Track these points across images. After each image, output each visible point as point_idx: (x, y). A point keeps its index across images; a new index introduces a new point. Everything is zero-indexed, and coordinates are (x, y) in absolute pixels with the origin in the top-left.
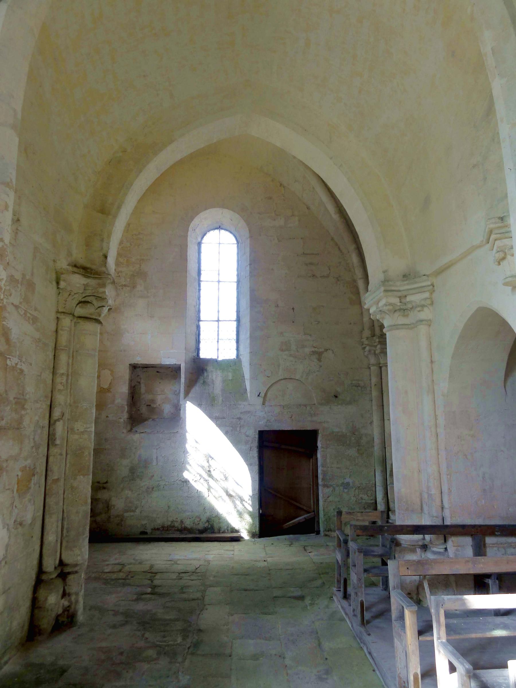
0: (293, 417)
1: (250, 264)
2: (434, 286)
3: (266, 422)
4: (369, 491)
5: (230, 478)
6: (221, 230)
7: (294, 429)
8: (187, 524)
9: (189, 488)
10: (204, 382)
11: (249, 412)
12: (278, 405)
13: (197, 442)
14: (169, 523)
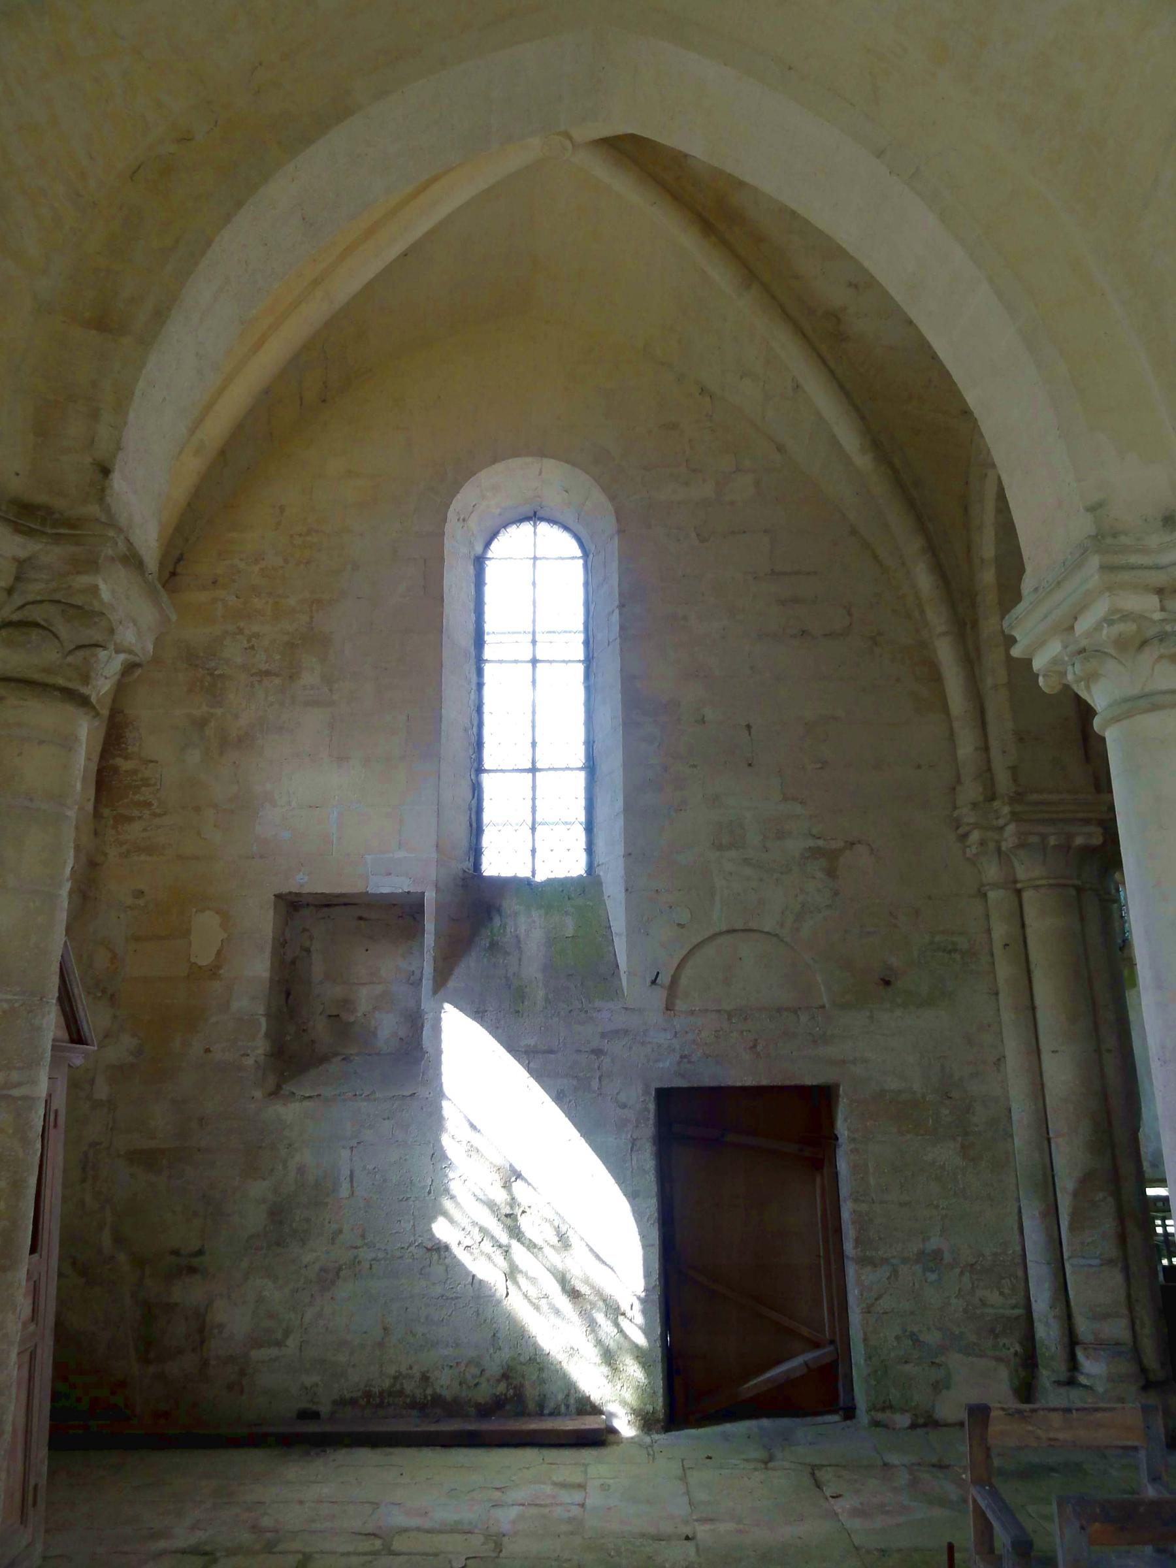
0: (759, 1048)
1: (622, 606)
3: (679, 1063)
4: (1004, 1278)
5: (574, 1240)
6: (538, 522)
8: (442, 1386)
9: (447, 1270)
10: (494, 947)
12: (714, 1011)
13: (473, 1127)
14: (387, 1383)
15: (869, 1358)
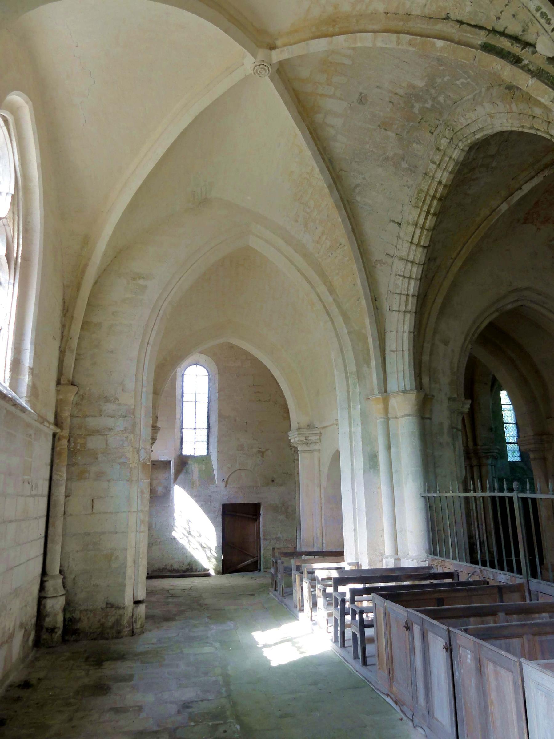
1: (218, 392)
2: (321, 433)
7: (246, 502)
10: (186, 472)
11: (216, 492)
14: (163, 567)
15: (264, 559)
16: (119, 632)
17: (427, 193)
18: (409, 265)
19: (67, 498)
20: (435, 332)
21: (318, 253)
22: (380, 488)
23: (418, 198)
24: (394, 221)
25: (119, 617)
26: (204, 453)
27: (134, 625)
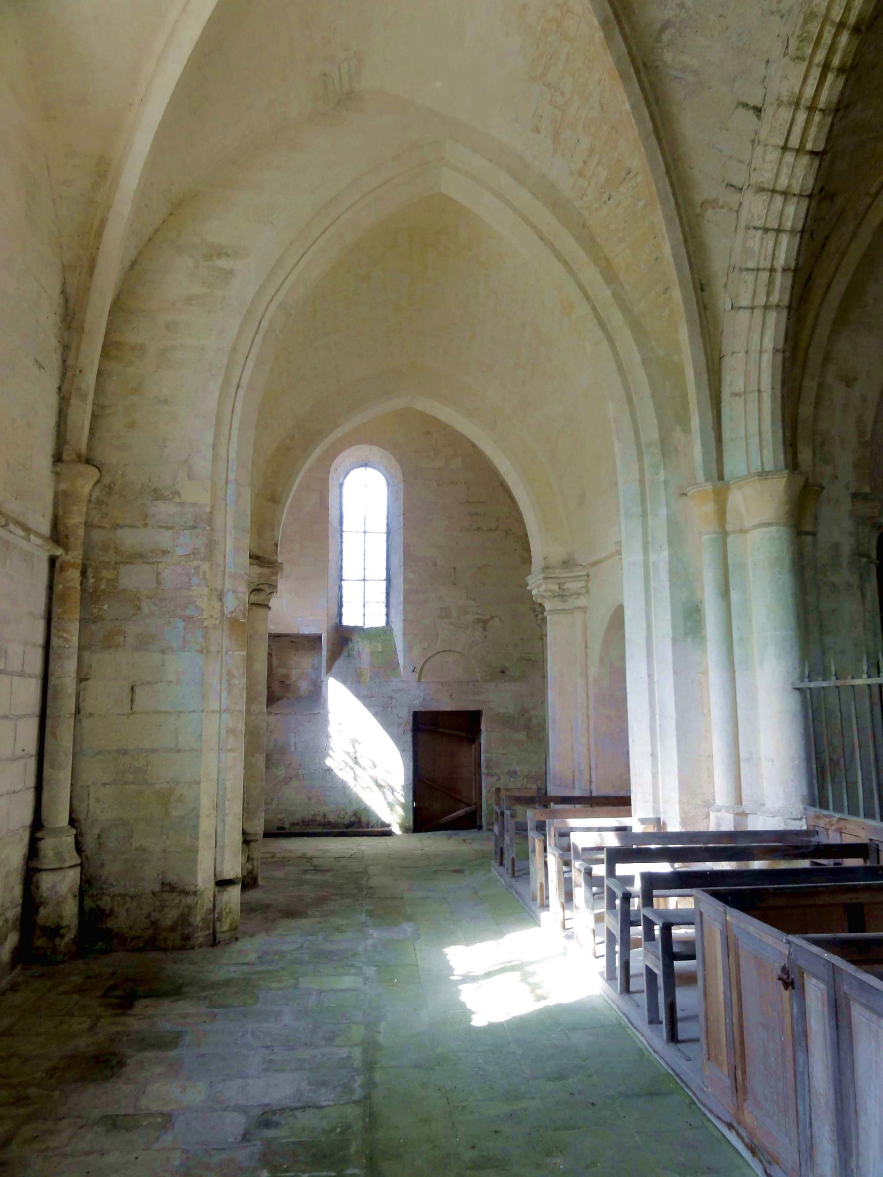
0: (453, 696)
1: (404, 514)
2: (588, 576)
3: (422, 702)
7: (454, 710)
10: (349, 656)
11: (402, 690)
14: (311, 817)
16: (187, 938)
17: (826, 18)
18: (779, 200)
19: (83, 684)
20: (827, 358)
21: (582, 199)
22: (705, 673)
23: (805, 35)
24: (745, 105)
25: (186, 910)
26: (381, 622)
27: (218, 925)
